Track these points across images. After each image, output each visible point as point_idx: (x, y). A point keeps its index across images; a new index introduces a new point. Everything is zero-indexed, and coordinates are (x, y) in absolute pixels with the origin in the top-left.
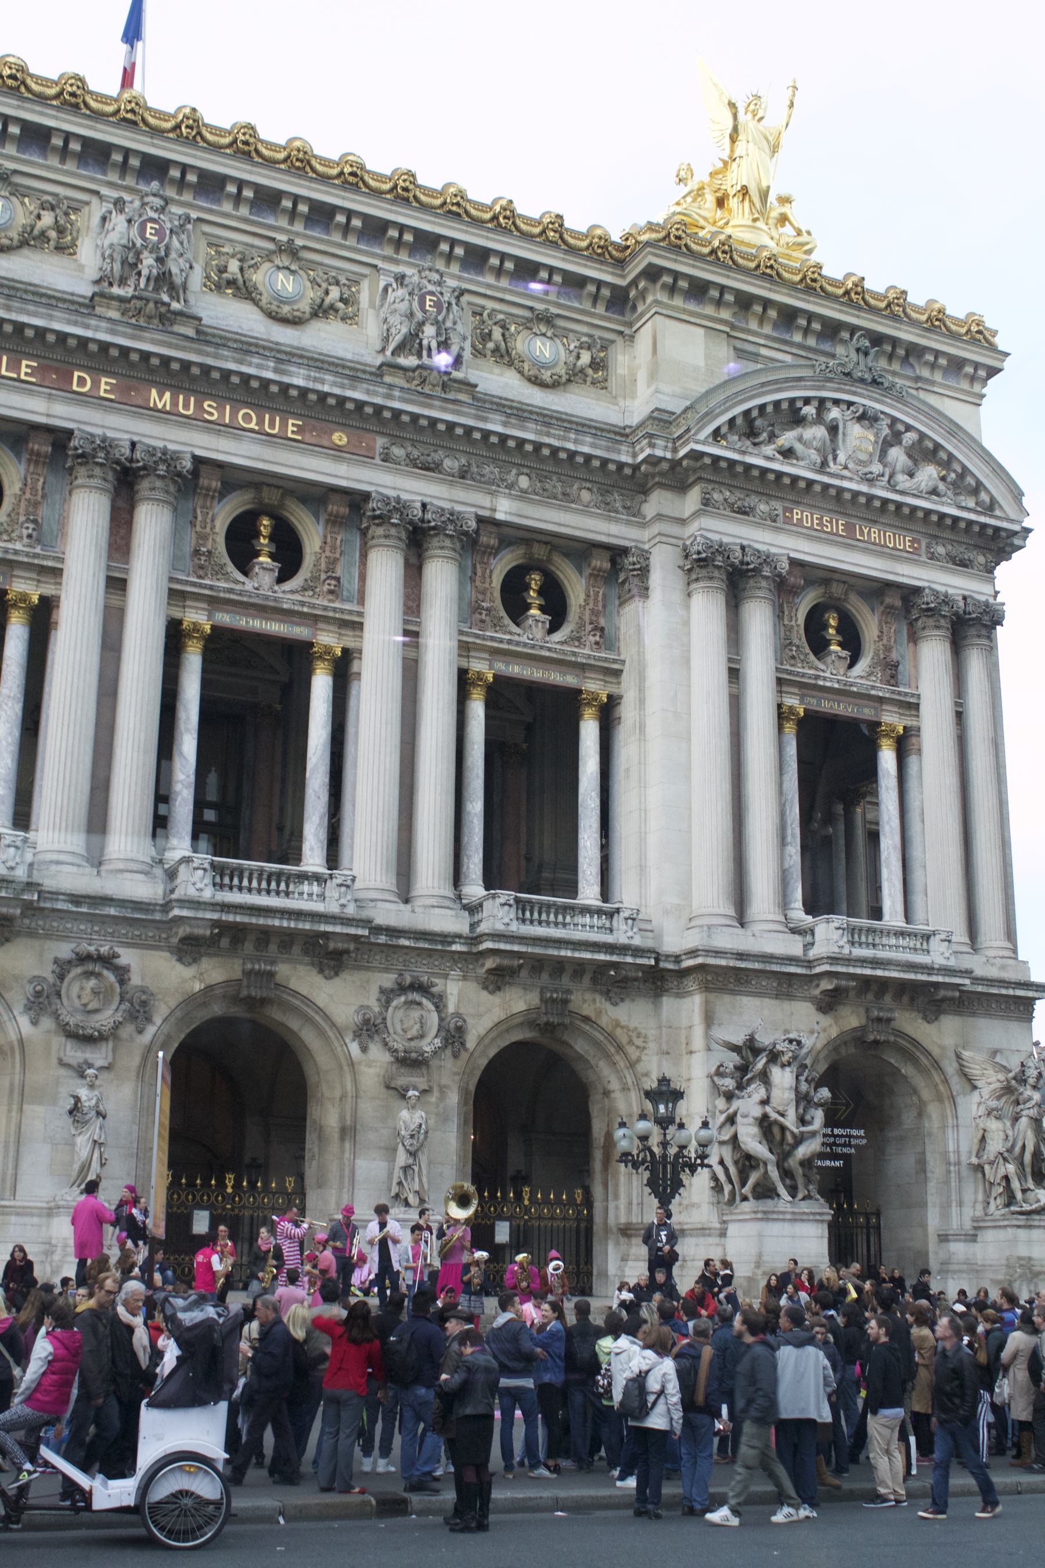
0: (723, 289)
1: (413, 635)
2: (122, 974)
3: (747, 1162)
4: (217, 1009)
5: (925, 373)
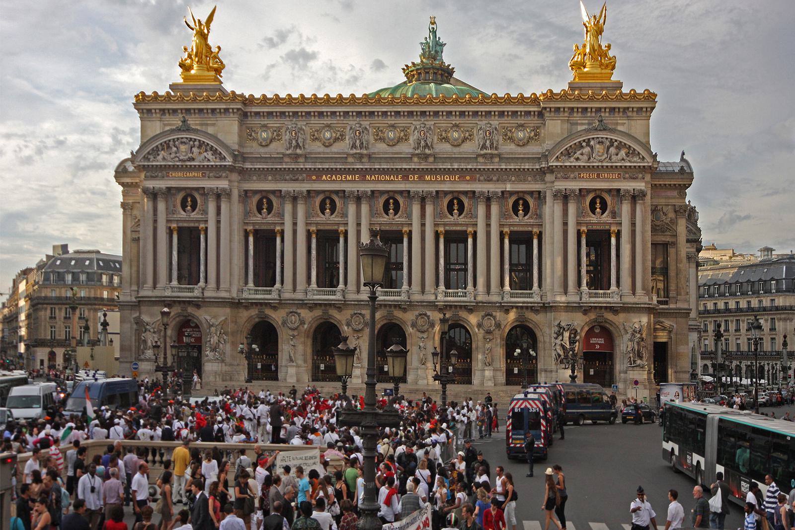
2: (428, 317)
5: (630, 114)
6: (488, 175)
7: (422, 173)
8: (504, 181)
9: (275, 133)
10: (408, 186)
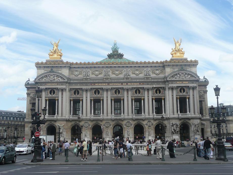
0: (171, 65)
1: (148, 97)
3: (173, 132)
4: (137, 124)
5: (191, 66)
6: (148, 83)
7: (127, 83)
8: (153, 85)
9: (80, 73)
10: (123, 86)
